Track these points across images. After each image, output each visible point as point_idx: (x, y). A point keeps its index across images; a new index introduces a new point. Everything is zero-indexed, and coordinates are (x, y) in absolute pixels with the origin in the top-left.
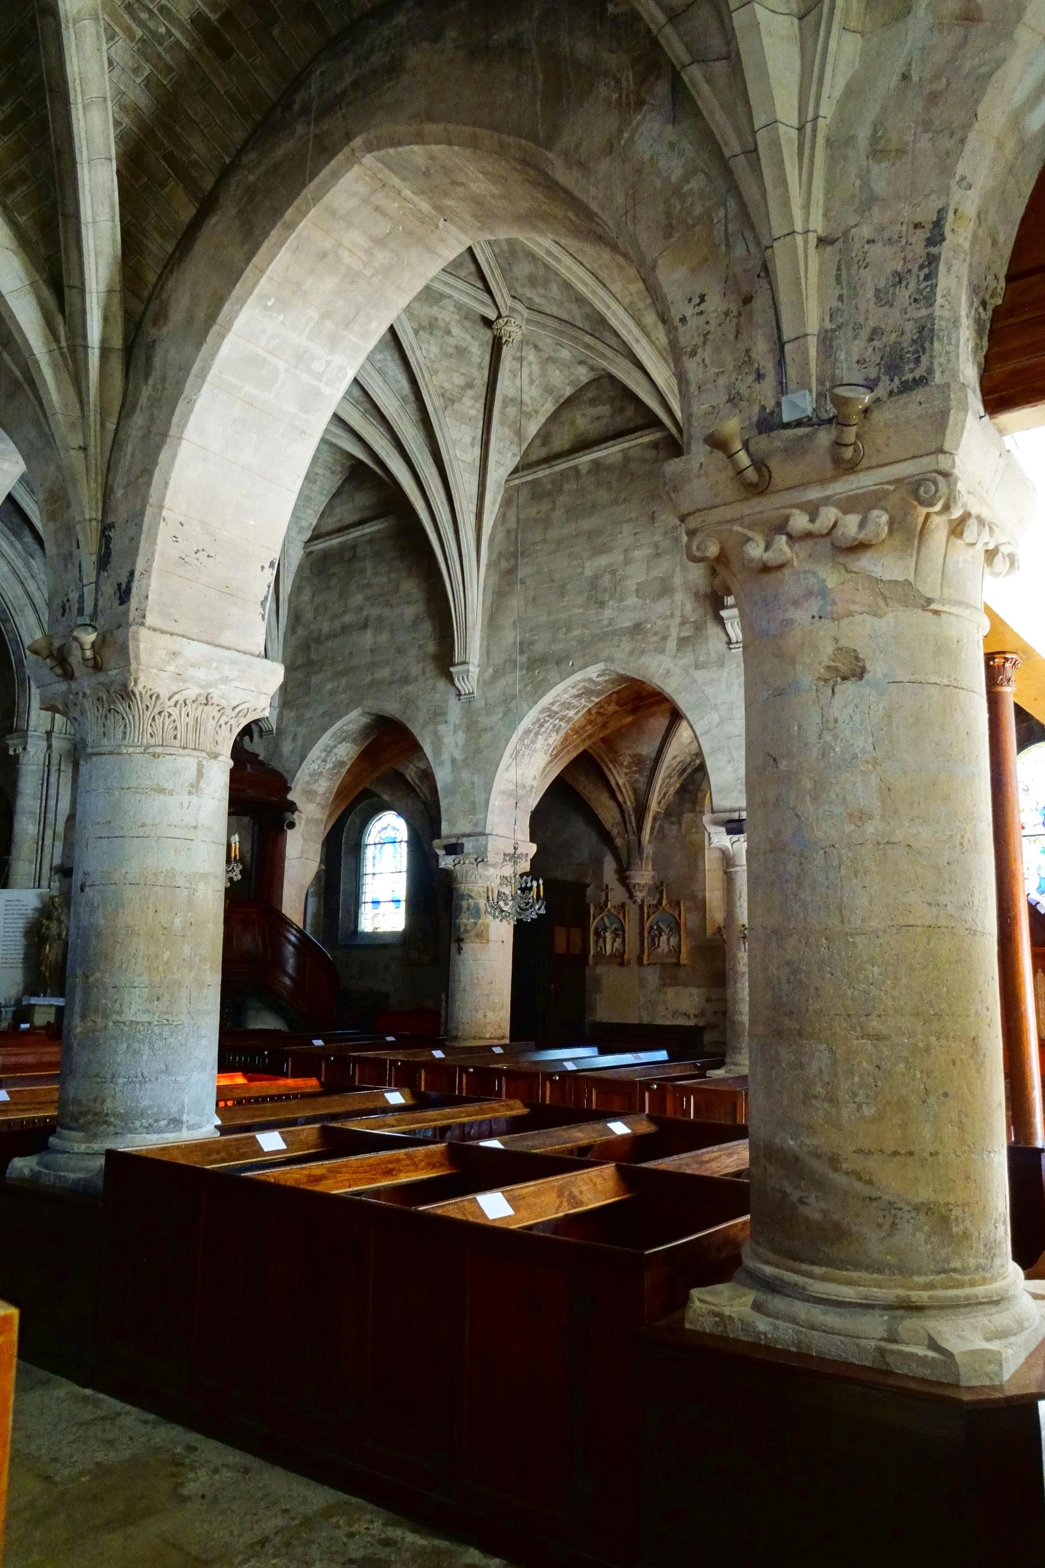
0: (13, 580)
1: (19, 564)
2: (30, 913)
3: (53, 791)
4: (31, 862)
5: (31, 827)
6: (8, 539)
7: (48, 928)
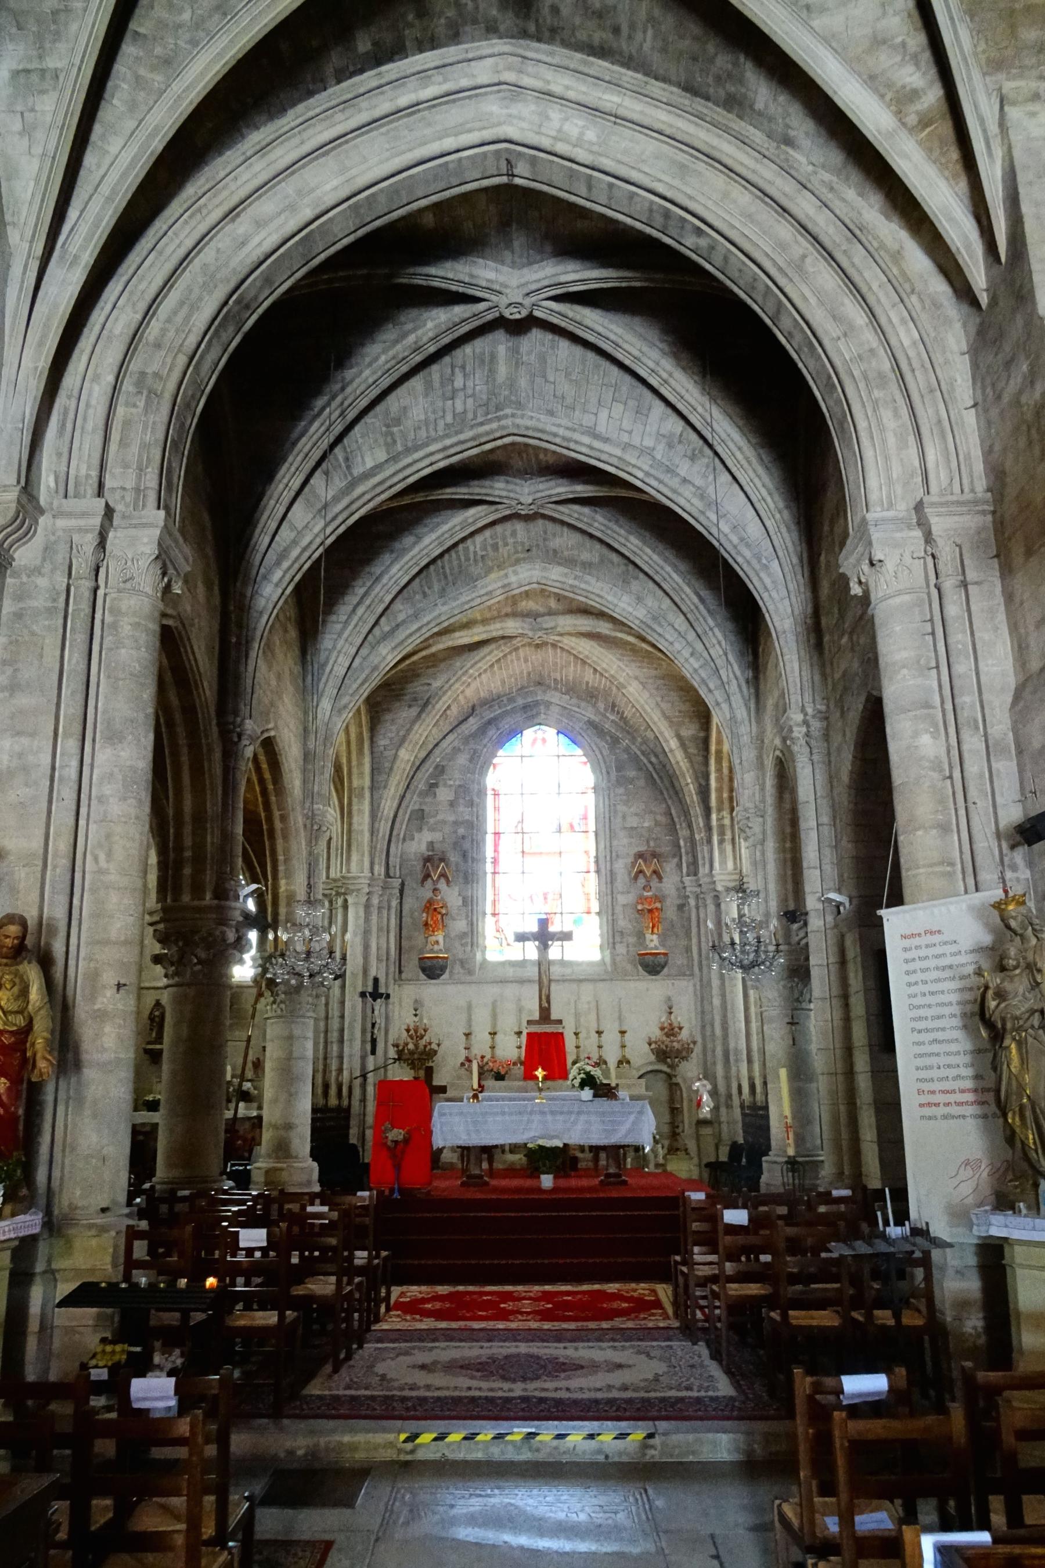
0: (766, 214)
1: (767, 174)
2: (967, 963)
3: (959, 638)
4: (944, 828)
5: (926, 739)
6: (727, 130)
7: (1001, 995)
